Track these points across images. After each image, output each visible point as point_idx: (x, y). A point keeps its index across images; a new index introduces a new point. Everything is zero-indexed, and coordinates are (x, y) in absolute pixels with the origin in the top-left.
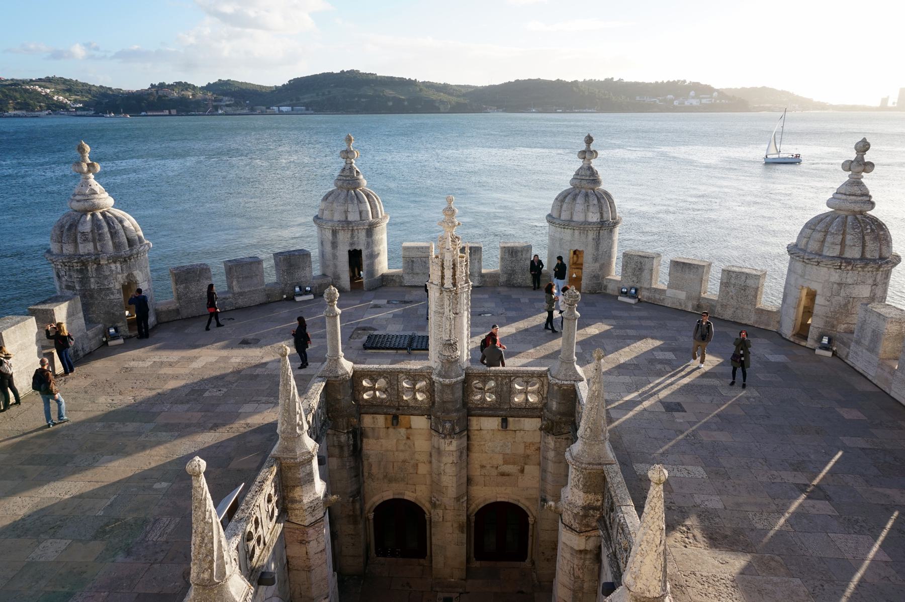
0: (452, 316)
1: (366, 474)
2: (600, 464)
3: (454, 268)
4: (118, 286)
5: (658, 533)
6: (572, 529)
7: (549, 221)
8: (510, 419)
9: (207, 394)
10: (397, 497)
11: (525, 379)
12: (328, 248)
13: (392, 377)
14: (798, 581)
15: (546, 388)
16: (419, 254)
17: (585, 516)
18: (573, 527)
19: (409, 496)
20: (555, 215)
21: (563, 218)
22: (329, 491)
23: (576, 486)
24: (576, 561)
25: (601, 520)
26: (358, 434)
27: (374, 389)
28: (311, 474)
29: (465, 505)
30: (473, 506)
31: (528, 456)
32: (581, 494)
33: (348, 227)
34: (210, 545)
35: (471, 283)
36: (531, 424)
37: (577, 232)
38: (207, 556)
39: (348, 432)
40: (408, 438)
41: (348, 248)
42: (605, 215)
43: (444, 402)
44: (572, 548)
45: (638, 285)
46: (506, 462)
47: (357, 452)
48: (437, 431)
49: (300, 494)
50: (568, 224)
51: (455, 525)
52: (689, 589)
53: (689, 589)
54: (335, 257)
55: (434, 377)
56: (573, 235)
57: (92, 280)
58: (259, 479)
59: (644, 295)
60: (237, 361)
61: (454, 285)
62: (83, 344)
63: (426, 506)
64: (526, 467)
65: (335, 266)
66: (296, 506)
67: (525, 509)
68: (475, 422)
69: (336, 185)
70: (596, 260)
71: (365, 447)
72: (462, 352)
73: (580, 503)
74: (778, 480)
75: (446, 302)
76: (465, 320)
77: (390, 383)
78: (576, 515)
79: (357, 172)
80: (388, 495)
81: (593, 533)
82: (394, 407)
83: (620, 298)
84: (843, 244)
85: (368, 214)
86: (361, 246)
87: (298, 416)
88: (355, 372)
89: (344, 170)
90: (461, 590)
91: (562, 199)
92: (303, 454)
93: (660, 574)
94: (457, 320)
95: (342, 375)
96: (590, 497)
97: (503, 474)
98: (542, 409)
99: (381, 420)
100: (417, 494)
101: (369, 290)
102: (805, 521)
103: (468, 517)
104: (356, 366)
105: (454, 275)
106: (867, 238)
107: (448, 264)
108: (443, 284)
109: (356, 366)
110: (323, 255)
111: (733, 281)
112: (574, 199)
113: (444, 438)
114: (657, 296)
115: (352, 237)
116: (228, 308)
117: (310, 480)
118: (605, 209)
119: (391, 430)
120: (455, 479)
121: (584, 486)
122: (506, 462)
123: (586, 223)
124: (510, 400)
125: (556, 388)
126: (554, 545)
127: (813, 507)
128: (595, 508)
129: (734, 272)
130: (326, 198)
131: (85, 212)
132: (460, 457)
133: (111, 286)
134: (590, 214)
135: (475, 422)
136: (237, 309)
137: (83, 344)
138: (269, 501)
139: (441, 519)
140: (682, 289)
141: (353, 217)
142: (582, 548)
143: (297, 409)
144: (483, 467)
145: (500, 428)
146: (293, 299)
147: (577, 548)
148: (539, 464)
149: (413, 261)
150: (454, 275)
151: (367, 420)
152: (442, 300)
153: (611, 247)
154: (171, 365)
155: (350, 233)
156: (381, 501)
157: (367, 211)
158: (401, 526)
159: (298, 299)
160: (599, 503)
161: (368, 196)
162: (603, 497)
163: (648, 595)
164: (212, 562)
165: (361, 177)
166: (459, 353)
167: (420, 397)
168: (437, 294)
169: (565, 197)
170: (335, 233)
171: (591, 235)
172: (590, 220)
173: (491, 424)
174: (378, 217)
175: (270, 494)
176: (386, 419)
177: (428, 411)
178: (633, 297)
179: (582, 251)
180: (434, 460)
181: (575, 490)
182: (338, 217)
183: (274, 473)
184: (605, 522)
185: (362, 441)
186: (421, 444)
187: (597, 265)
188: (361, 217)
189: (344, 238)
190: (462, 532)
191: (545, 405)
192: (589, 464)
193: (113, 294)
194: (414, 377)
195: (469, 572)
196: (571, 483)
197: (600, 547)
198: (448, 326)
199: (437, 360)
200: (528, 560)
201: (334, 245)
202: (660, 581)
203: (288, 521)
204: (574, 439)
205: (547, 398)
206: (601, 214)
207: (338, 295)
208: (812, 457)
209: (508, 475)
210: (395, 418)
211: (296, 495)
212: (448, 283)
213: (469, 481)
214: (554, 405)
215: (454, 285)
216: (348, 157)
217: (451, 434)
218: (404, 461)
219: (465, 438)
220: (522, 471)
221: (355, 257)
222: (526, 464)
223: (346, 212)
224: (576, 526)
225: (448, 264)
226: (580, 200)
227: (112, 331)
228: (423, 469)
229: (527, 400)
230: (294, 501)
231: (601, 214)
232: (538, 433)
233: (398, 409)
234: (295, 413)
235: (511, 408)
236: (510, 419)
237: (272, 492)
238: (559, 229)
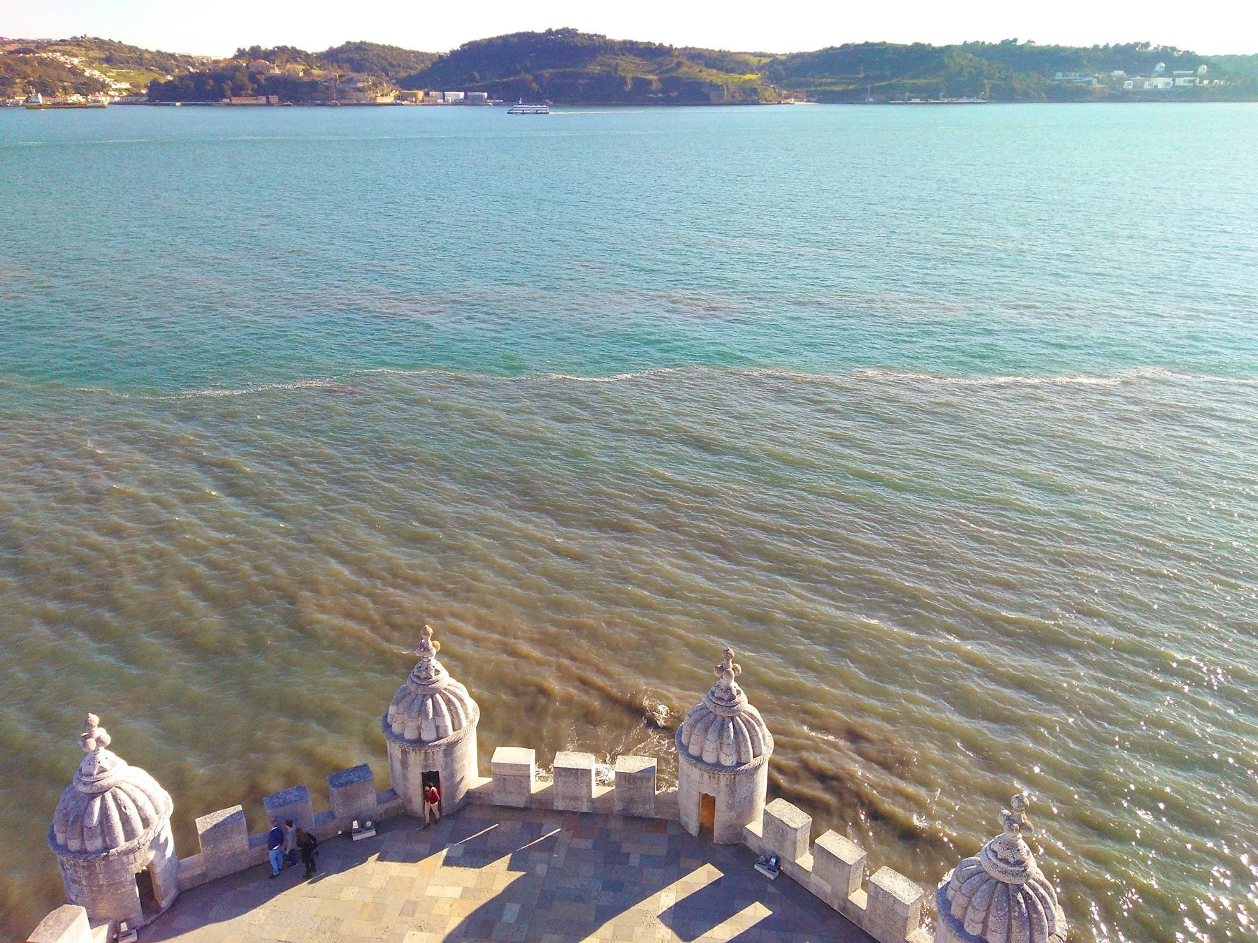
16: (513, 772)
45: (780, 854)
54: (405, 777)
56: (702, 776)
65: (406, 788)
70: (731, 807)
84: (985, 922)
106: (1014, 922)
111: (880, 897)
114: (802, 877)
115: (426, 758)
118: (743, 749)
123: (718, 766)
131: (93, 796)
140: (827, 880)
157: (446, 727)
170: (404, 753)
171: (723, 782)
172: (723, 763)
178: (770, 869)
182: (409, 735)
187: (733, 814)
201: (404, 764)
206: (739, 752)
223: (419, 728)
226: (712, 736)
231: (739, 752)
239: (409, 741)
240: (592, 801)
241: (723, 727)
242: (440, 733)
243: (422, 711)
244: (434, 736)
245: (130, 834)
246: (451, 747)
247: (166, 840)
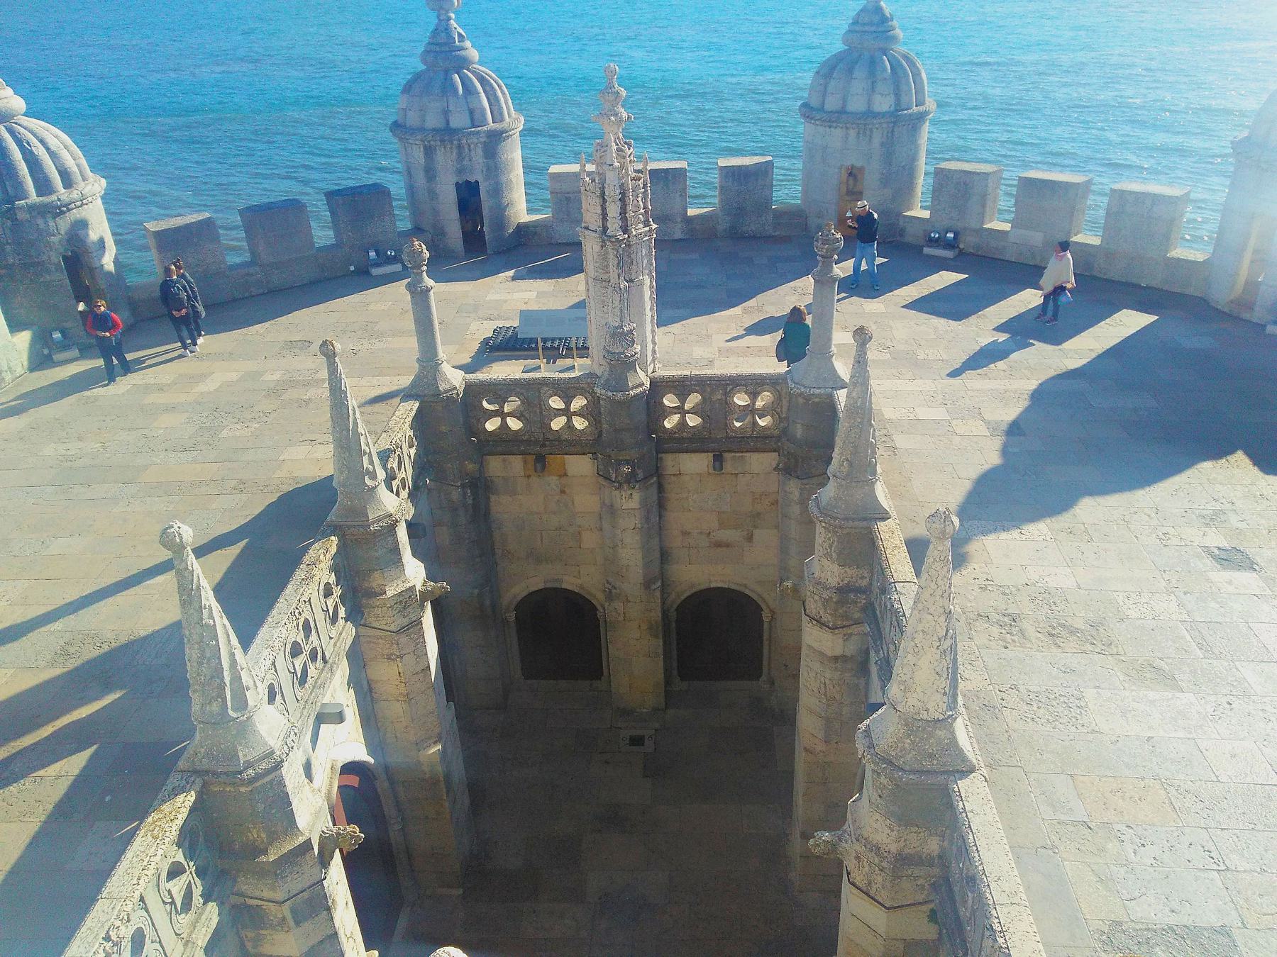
0: (624, 284)
1: (499, 552)
2: (865, 519)
3: (622, 200)
4: (56, 258)
5: (943, 619)
6: (822, 624)
7: (804, 116)
8: (727, 456)
9: (224, 433)
10: (549, 585)
11: (750, 388)
12: (420, 179)
13: (531, 392)
14: (1191, 697)
15: (785, 402)
17: (841, 603)
18: (824, 619)
19: (570, 583)
20: (815, 103)
21: (828, 107)
22: (430, 576)
23: (827, 556)
24: (828, 674)
25: (869, 609)
26: (480, 487)
27: (503, 416)
28: (396, 550)
29: (658, 594)
30: (673, 596)
31: (759, 514)
32: (836, 568)
33: (452, 143)
34: (214, 662)
35: (654, 226)
36: (761, 463)
37: (852, 133)
38: (212, 677)
39: (463, 486)
40: (563, 492)
41: (455, 180)
42: (904, 99)
43: (615, 430)
44: (822, 654)
46: (722, 525)
47: (480, 514)
48: (608, 479)
49: (380, 582)
50: (837, 118)
51: (644, 627)
52: (1006, 712)
53: (1006, 712)
54: (433, 194)
55: (598, 390)
57: (8, 248)
58: (307, 558)
59: (968, 242)
60: (277, 376)
61: (625, 230)
62: (8, 361)
63: (598, 597)
64: (756, 532)
66: (376, 601)
67: (755, 598)
68: (671, 462)
69: (424, 61)
71: (495, 508)
72: (644, 347)
73: (833, 581)
74: (1175, 541)
75: (613, 262)
76: (647, 293)
77: (527, 402)
78: (826, 602)
79: (460, 35)
80: (536, 584)
81: (855, 629)
82: (537, 442)
83: (927, 250)
85: (484, 115)
86: (477, 176)
87: (365, 459)
88: (469, 386)
89: (436, 32)
90: (657, 726)
91: (831, 70)
92: (379, 520)
93: (944, 684)
94: (633, 291)
95: (446, 391)
96: (851, 572)
97: (719, 545)
98: (779, 438)
99: (516, 463)
100: (582, 578)
101: (499, 253)
102: (1213, 604)
103: (665, 613)
104: (469, 377)
105: (623, 212)
107: (612, 192)
108: (605, 229)
109: (470, 377)
110: (411, 190)
112: (850, 71)
113: (617, 489)
115: (460, 157)
116: (255, 291)
117: (397, 561)
118: (904, 87)
119: (534, 479)
120: (640, 556)
121: (839, 555)
122: (722, 525)
123: (870, 114)
124: (726, 426)
125: (801, 400)
126: (796, 651)
127: (1230, 583)
128: (859, 590)
129: (1131, 193)
130: (407, 89)
132: (647, 519)
133: (45, 258)
134: (877, 99)
135: (671, 462)
136: (270, 292)
137: (8, 361)
138: (328, 593)
139: (621, 618)
141: (459, 120)
142: (838, 652)
143: (364, 447)
144: (685, 533)
145: (711, 471)
146: (367, 273)
147: (829, 654)
148: (777, 527)
149: (568, 199)
150: (623, 212)
151: (495, 466)
152: (605, 257)
153: (913, 159)
154: (161, 388)
155: (455, 151)
156: (525, 594)
157: (483, 109)
158: (559, 631)
159: (376, 271)
160: (865, 582)
161: (483, 80)
162: (872, 572)
163: (925, 716)
164: (222, 686)
165: (468, 44)
166: (638, 348)
167: (580, 424)
168: (597, 248)
169: (833, 68)
170: (429, 152)
171: (877, 139)
173: (695, 463)
174: (502, 120)
175: (328, 584)
176: (525, 462)
177: (591, 445)
178: (950, 245)
179: (861, 169)
180: (606, 526)
181: (825, 562)
182: (433, 121)
183: (334, 550)
184: (874, 611)
185: (488, 498)
186: (586, 500)
188: (472, 120)
189: (445, 160)
190: (656, 637)
191: (784, 431)
192: (847, 519)
193: (48, 271)
194: (567, 390)
195: (670, 697)
196: (819, 550)
197: (867, 652)
198: (617, 303)
199: (603, 362)
200: (764, 678)
202: (945, 694)
203: (365, 625)
204: (823, 480)
205: (787, 419)
206: (897, 95)
207: (428, 255)
208: (1239, 504)
209: (728, 546)
210: (541, 460)
211: (374, 585)
212: (614, 227)
213: (665, 556)
214: (799, 431)
215: (625, 230)
216: (441, 8)
217: (631, 480)
218: (559, 528)
219: (654, 490)
220: (750, 538)
221: (468, 198)
222: (755, 527)
223: (446, 113)
224: (827, 618)
225: (612, 192)
226: (860, 73)
227: (57, 335)
228: (590, 540)
229: (755, 423)
230: (372, 594)
231: (897, 95)
232: (774, 475)
233: (544, 445)
234: (361, 453)
235: (728, 437)
236: (727, 456)
237: (332, 579)
238: (821, 129)
239: (436, 131)
240: (689, 221)
241: (873, 64)
242: (475, 117)
243: (448, 88)
244: (469, 122)
245: (44, 186)
246: (497, 137)
247: (101, 242)
